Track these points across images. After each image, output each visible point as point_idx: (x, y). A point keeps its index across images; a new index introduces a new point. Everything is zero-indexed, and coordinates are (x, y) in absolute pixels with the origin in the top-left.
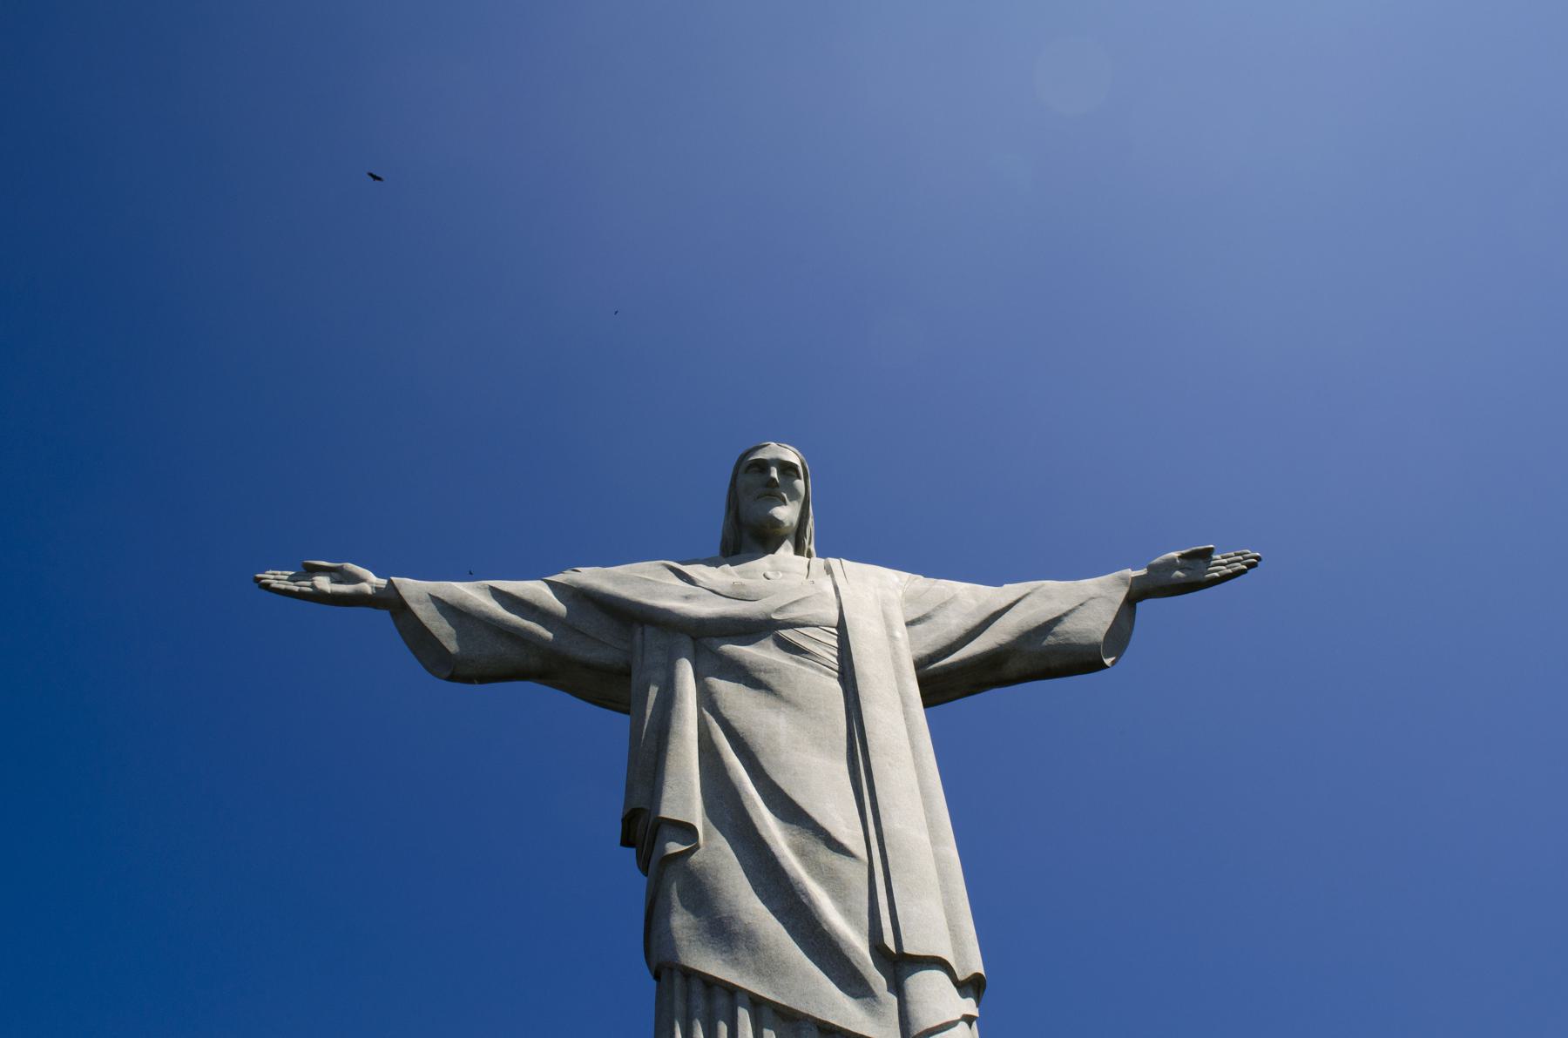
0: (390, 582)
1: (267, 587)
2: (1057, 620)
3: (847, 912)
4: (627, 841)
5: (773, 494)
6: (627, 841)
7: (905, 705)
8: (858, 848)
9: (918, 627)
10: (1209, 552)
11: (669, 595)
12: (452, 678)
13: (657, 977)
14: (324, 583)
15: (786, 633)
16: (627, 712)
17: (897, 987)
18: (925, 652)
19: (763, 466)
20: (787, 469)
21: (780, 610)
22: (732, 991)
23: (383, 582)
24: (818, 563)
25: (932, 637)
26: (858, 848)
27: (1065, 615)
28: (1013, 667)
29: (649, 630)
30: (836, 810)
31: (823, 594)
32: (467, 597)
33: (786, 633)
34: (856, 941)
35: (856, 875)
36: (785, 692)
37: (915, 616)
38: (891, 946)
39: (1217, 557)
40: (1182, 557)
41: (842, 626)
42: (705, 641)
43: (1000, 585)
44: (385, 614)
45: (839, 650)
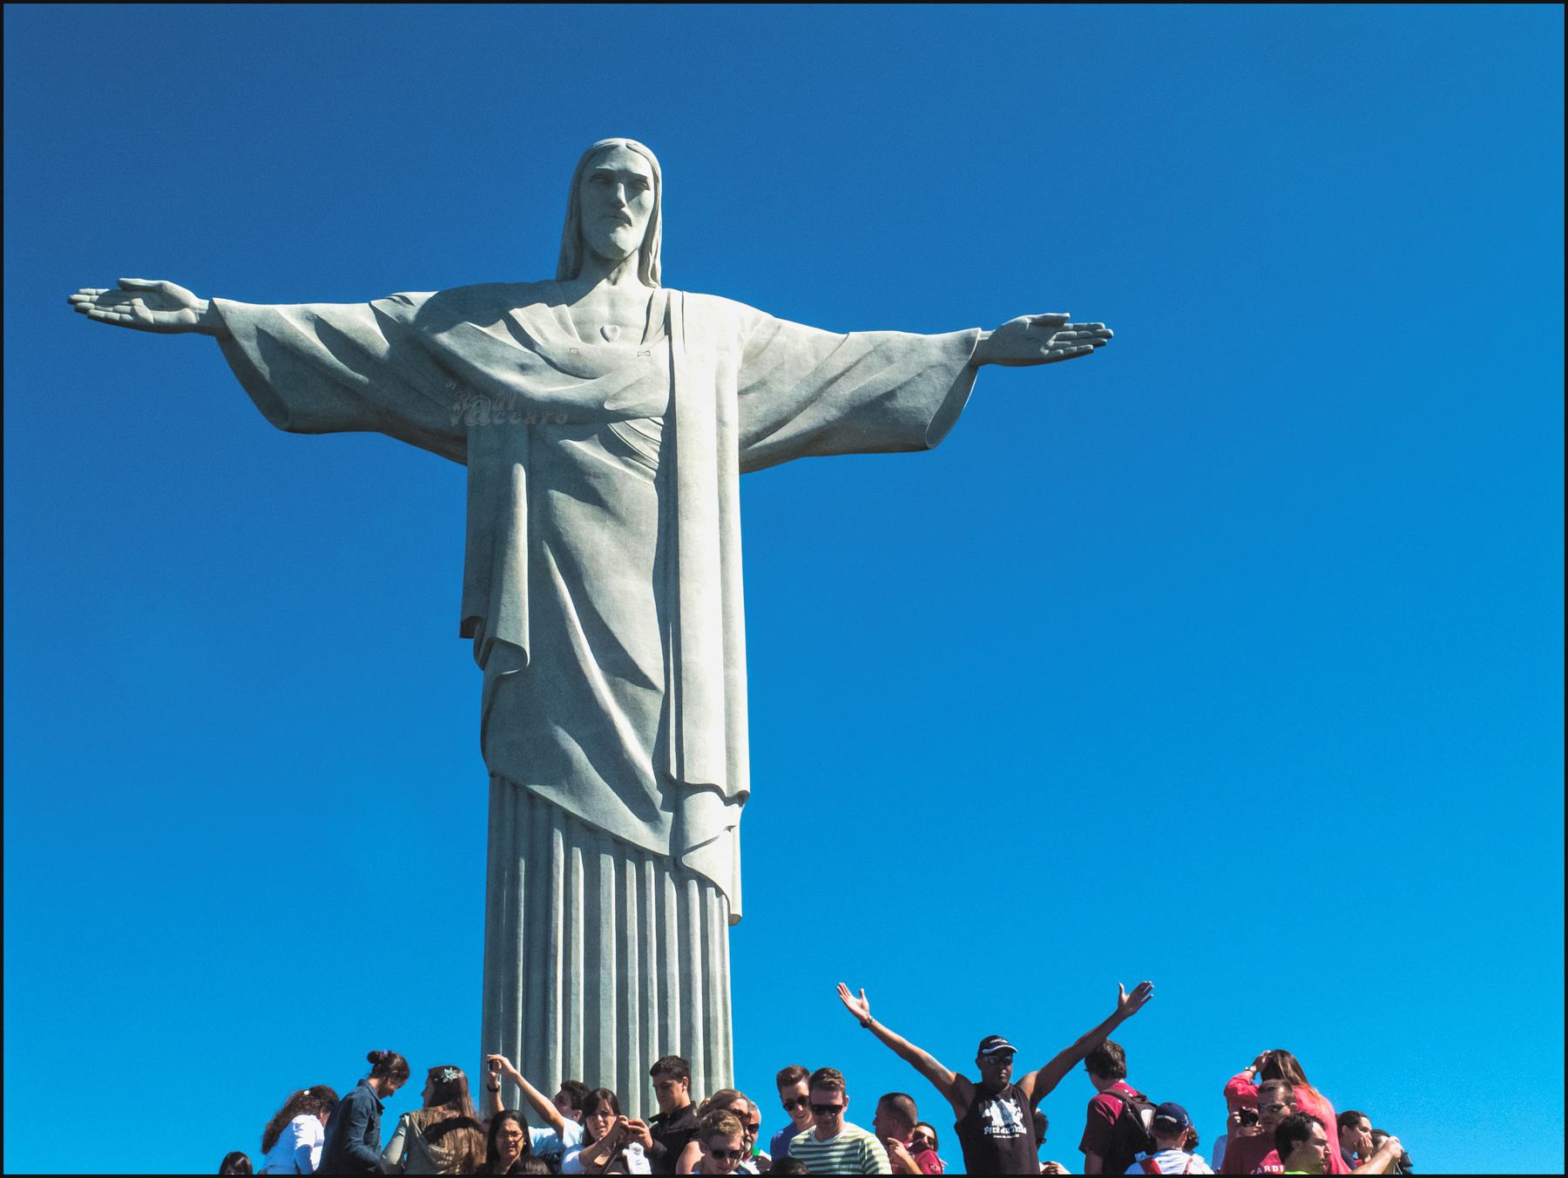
0: (212, 304)
1: (85, 311)
2: (891, 395)
3: (644, 740)
4: (466, 632)
6: (466, 632)
7: (722, 510)
8: (659, 681)
9: (752, 396)
11: (504, 362)
12: (291, 430)
13: (492, 775)
15: (616, 427)
16: (465, 463)
18: (753, 429)
20: (636, 184)
21: (615, 398)
23: (203, 304)
24: (661, 294)
26: (659, 681)
27: (900, 388)
30: (643, 643)
31: (657, 373)
32: (297, 334)
33: (616, 427)
35: (652, 704)
36: (611, 501)
37: (749, 383)
40: (1035, 323)
41: (670, 418)
43: (846, 331)
44: (213, 340)
45: (662, 445)
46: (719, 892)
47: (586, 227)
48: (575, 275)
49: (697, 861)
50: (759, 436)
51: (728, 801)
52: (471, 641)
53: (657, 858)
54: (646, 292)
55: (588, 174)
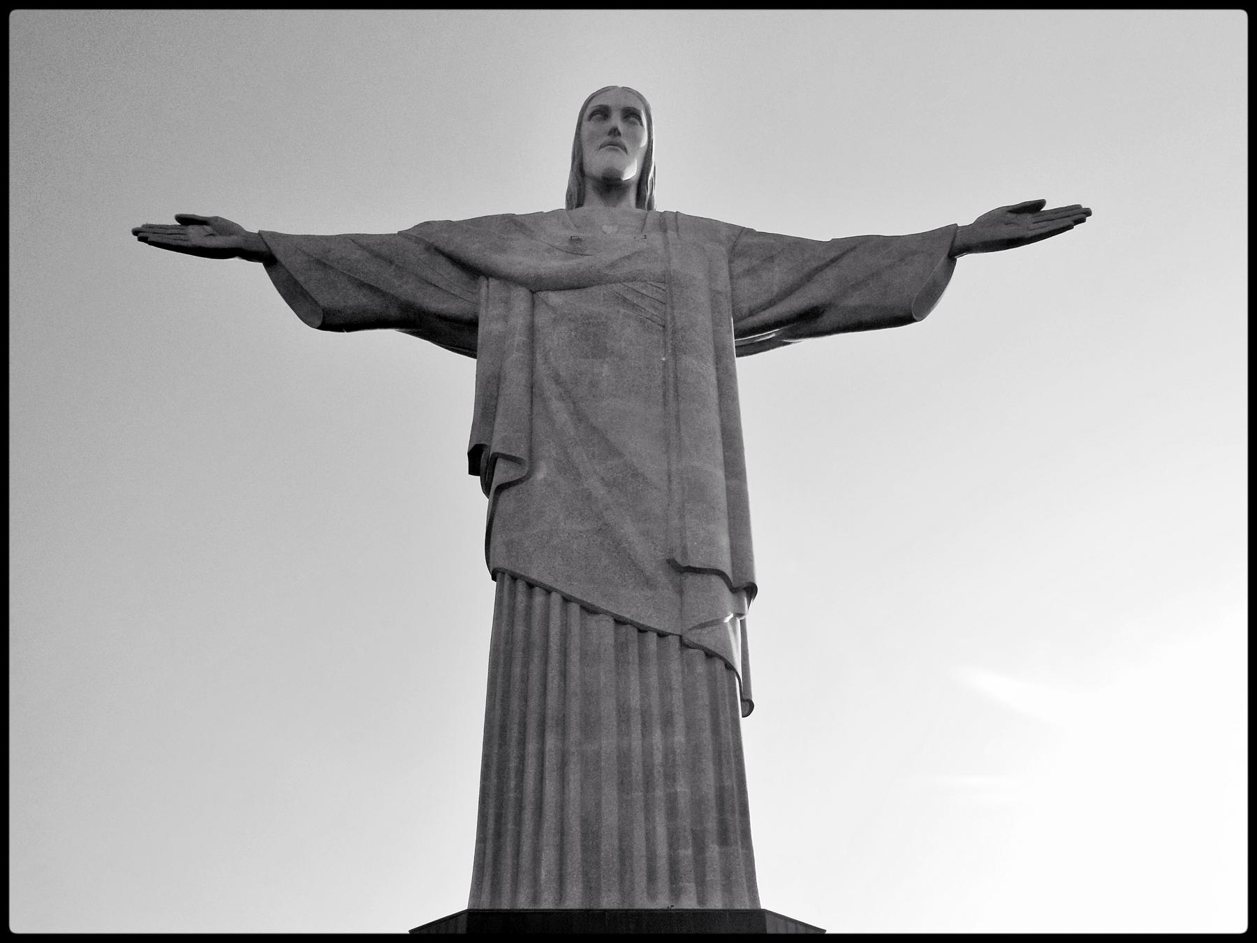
13: (494, 578)
14: (195, 235)
17: (681, 592)
21: (613, 265)
22: (548, 591)
25: (752, 292)
29: (493, 283)
33: (617, 287)
34: (648, 554)
38: (679, 560)
42: (542, 294)
46: (730, 667)
47: (587, 159)
48: (579, 205)
50: (752, 313)
51: (734, 590)
52: (477, 480)
53: (662, 635)
54: (639, 211)
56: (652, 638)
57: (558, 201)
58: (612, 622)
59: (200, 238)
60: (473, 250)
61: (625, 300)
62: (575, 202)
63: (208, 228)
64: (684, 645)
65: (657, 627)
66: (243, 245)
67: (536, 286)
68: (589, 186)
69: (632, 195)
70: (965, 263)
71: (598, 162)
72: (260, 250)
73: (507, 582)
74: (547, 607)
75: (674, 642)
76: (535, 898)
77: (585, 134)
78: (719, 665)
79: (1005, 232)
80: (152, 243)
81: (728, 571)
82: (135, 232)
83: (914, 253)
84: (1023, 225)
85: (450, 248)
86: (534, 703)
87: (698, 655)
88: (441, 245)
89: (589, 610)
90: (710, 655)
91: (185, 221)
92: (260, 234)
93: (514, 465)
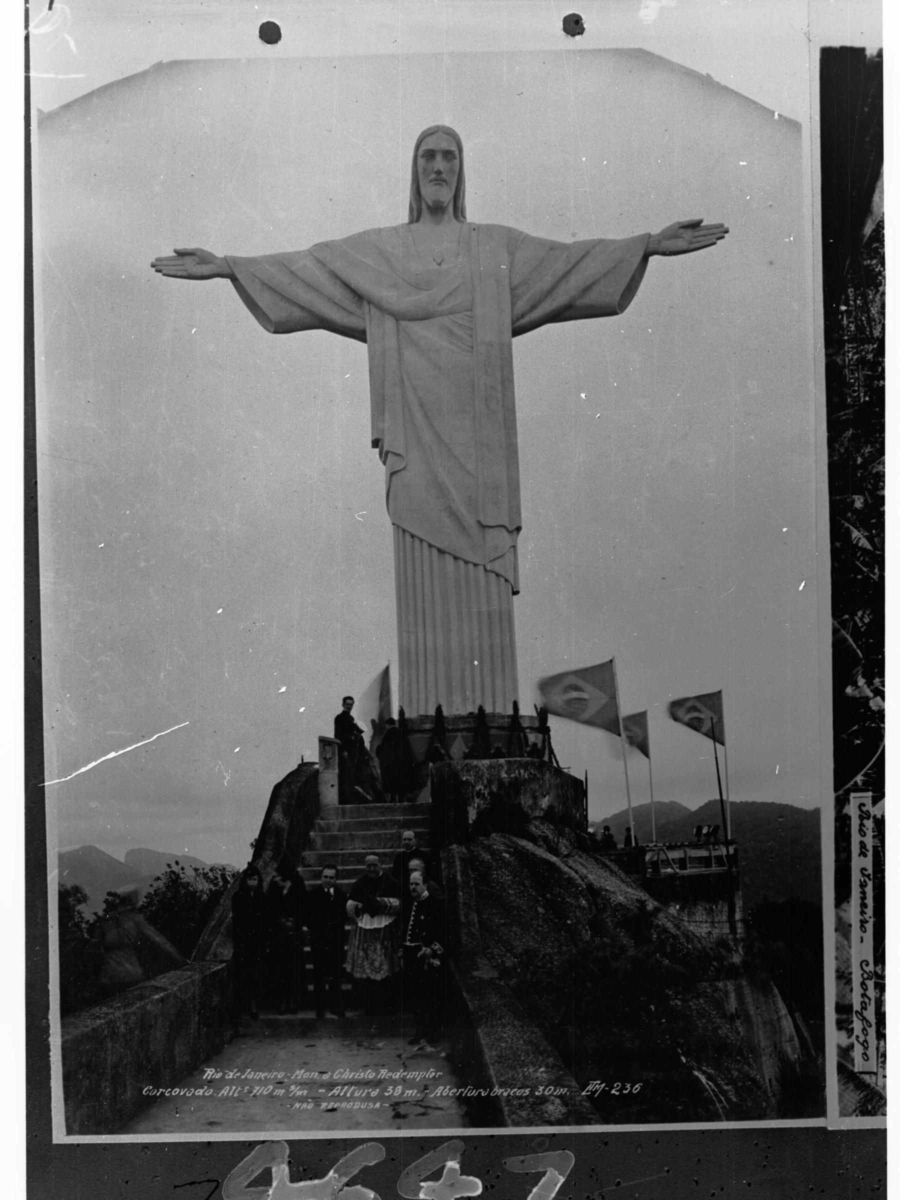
5: (439, 179)
10: (701, 221)
12: (275, 332)
14: (190, 265)
19: (430, 155)
21: (441, 303)
22: (421, 540)
28: (567, 314)
29: (373, 310)
33: (446, 320)
39: (702, 224)
42: (403, 323)
44: (228, 281)
46: (506, 580)
48: (418, 220)
49: (497, 566)
53: (475, 565)
55: (420, 152)
56: (471, 566)
57: (404, 216)
58: (452, 559)
59: (190, 265)
60: (360, 281)
61: (450, 332)
62: (415, 215)
63: (193, 257)
64: (485, 570)
65: (474, 561)
66: (217, 272)
67: (398, 317)
68: (424, 206)
69: (451, 209)
70: (654, 260)
71: (429, 192)
72: (229, 271)
73: (401, 532)
74: (422, 549)
75: (481, 568)
76: (426, 711)
77: (420, 170)
78: (503, 580)
79: (681, 244)
80: (164, 275)
81: (507, 525)
82: (153, 266)
83: (621, 261)
84: (693, 236)
85: (344, 276)
86: (419, 604)
87: (493, 576)
88: (339, 274)
89: (441, 552)
90: (498, 575)
91: (181, 254)
92: (225, 258)
93: (398, 458)
